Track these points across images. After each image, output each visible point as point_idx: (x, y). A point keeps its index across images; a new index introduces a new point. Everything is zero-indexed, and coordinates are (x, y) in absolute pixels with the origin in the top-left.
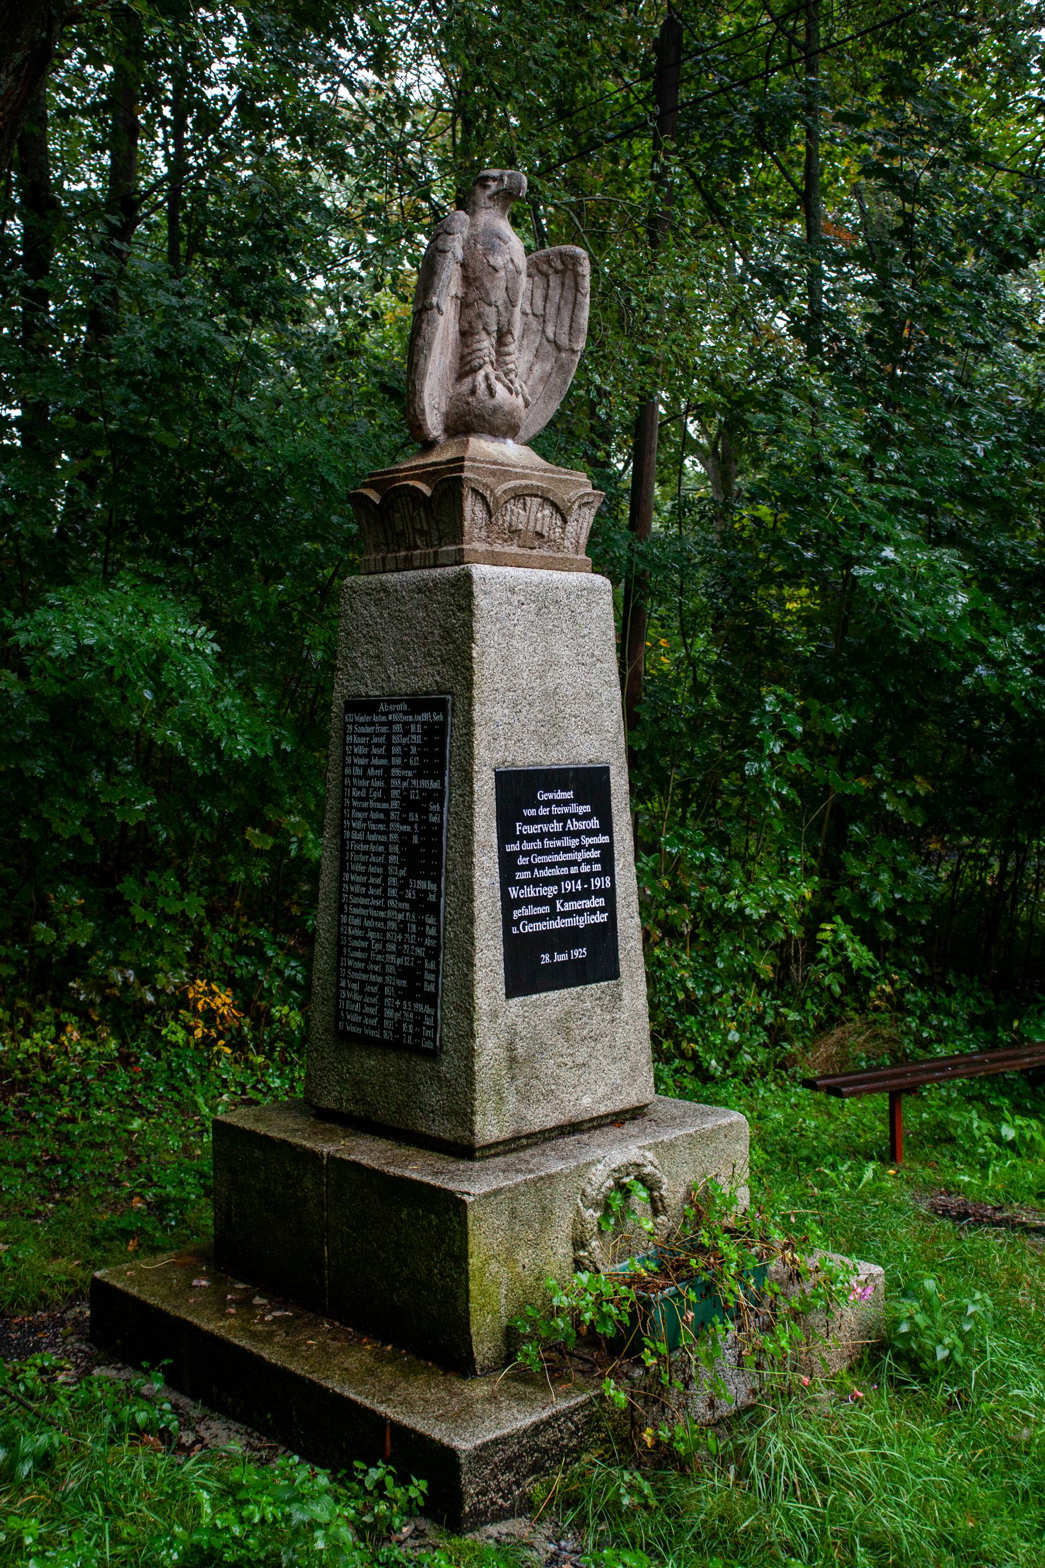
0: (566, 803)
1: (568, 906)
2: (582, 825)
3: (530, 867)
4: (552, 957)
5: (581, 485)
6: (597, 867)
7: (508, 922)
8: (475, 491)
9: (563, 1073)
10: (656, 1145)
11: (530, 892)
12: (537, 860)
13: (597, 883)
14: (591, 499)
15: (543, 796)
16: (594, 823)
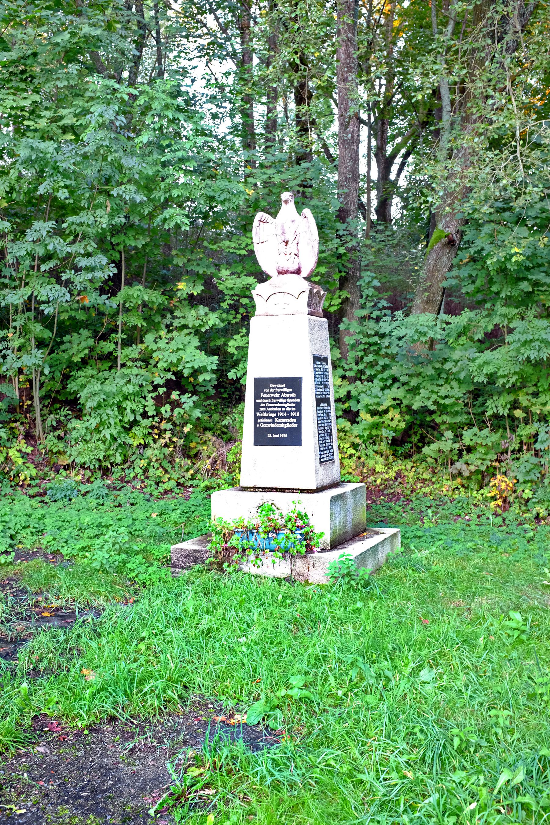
1: (280, 420)
2: (288, 395)
3: (266, 407)
6: (294, 409)
7: (256, 423)
11: (265, 415)
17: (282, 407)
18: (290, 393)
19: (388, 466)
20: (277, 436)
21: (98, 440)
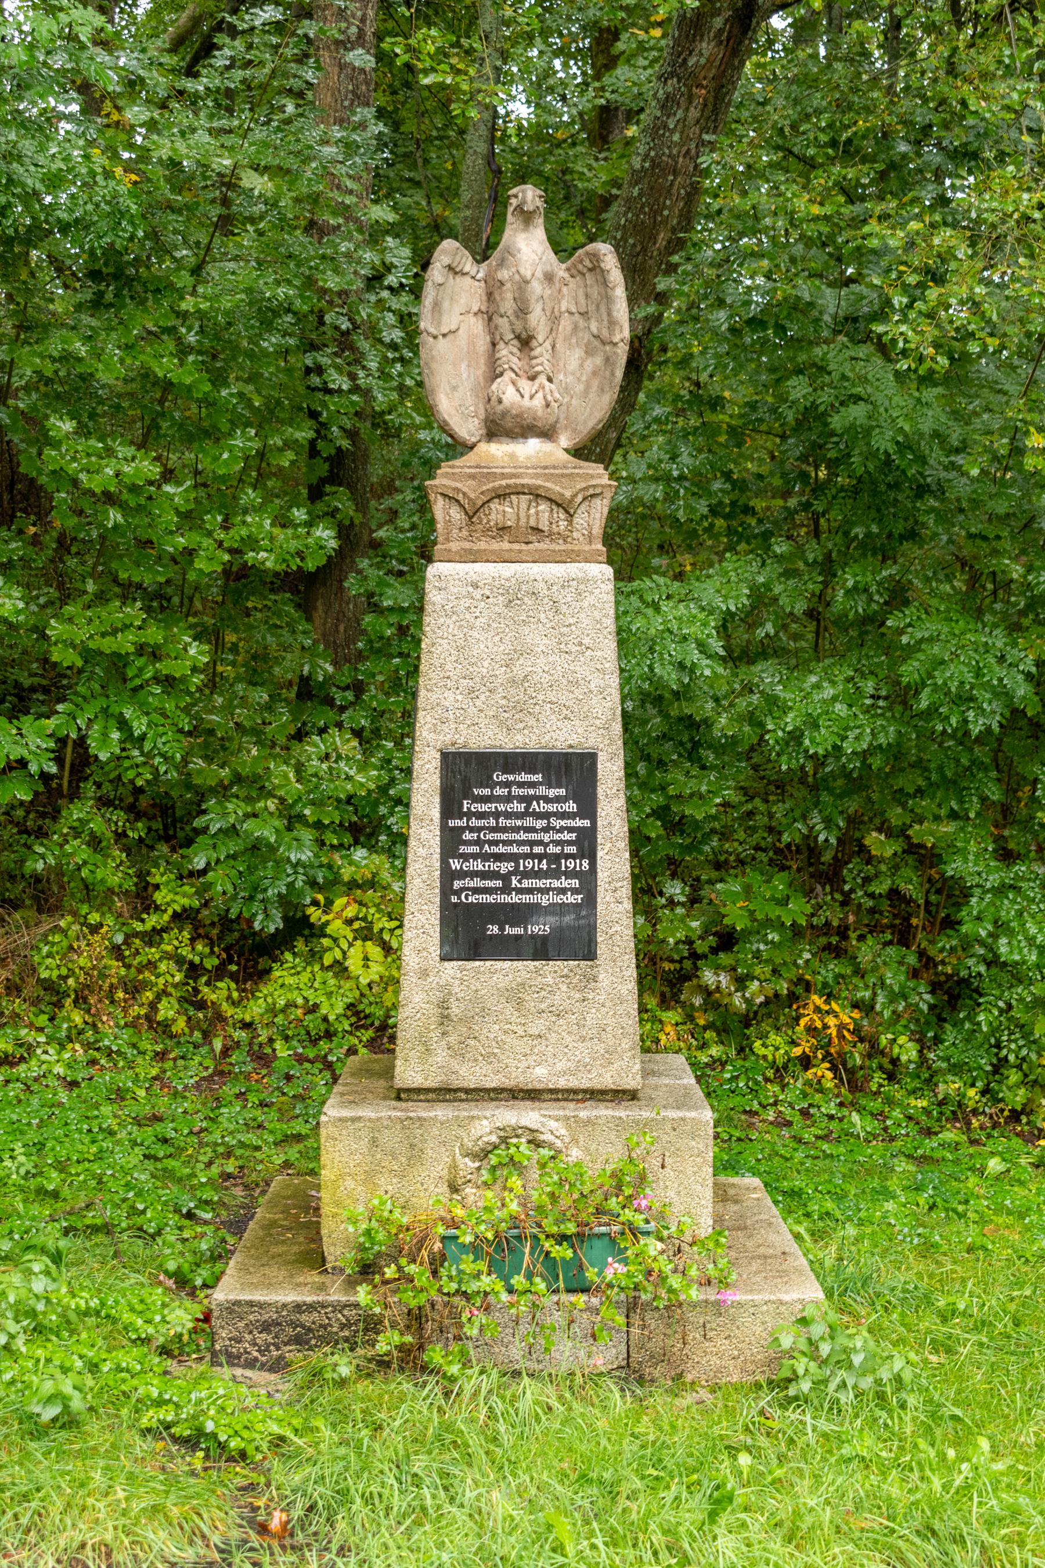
0: (532, 785)
1: (526, 883)
2: (552, 808)
3: (478, 842)
4: (502, 929)
5: (600, 476)
6: (573, 850)
7: (446, 890)
8: (444, 495)
9: (509, 1039)
11: (479, 866)
12: (490, 837)
14: (598, 491)
17: (532, 843)
18: (558, 799)
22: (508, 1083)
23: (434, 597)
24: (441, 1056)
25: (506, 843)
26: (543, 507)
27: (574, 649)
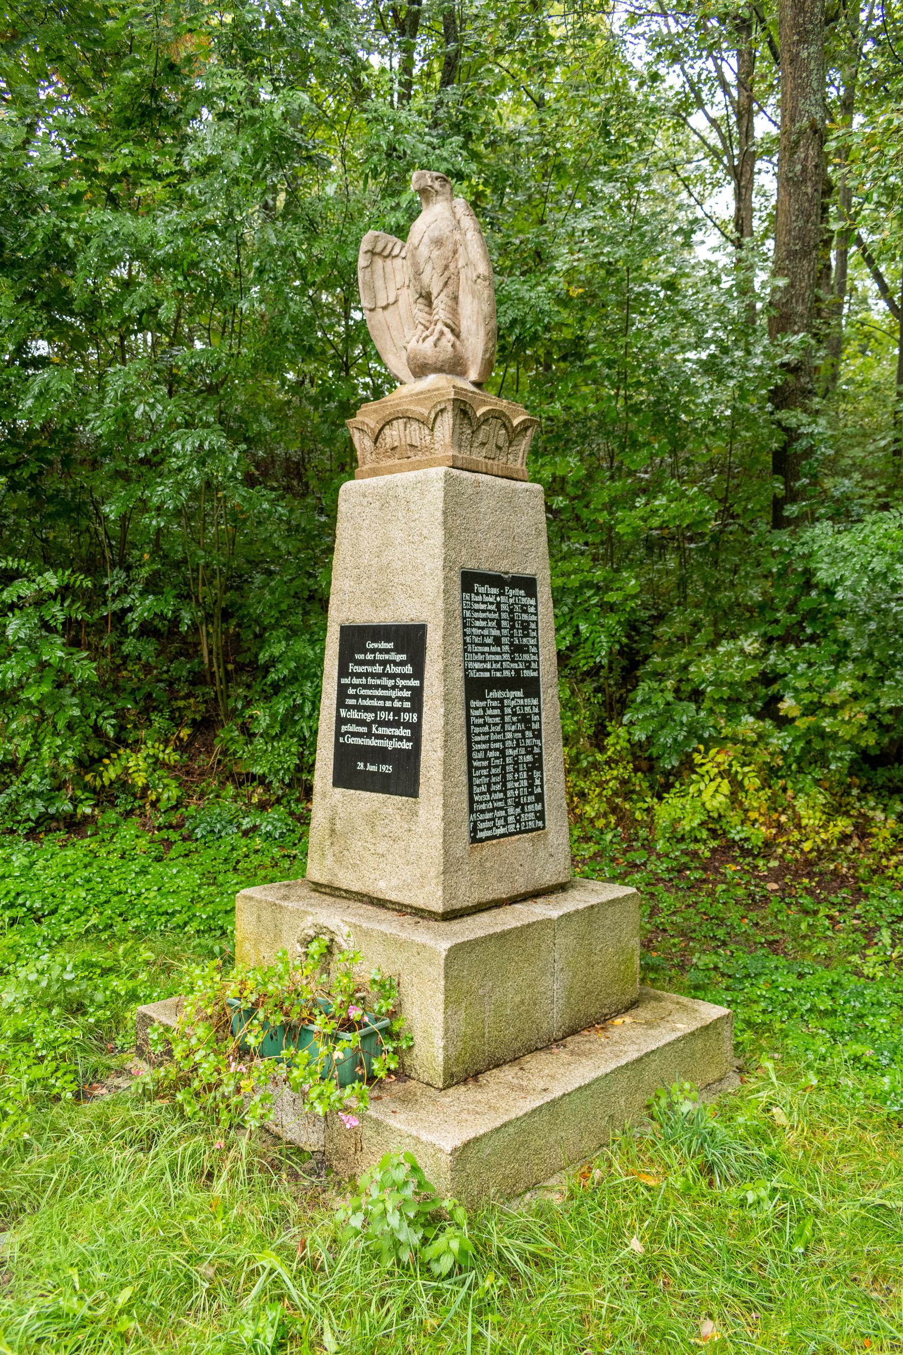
0: (387, 651)
2: (398, 670)
3: (356, 697)
6: (407, 705)
7: (338, 734)
9: (366, 854)
10: (356, 926)
11: (354, 714)
13: (406, 717)
15: (371, 645)
16: (408, 669)
19: (835, 810)
20: (372, 768)
21: (292, 737)
22: (364, 890)
23: (343, 507)
24: (329, 861)
25: (372, 698)
26: (415, 425)
27: (416, 538)
